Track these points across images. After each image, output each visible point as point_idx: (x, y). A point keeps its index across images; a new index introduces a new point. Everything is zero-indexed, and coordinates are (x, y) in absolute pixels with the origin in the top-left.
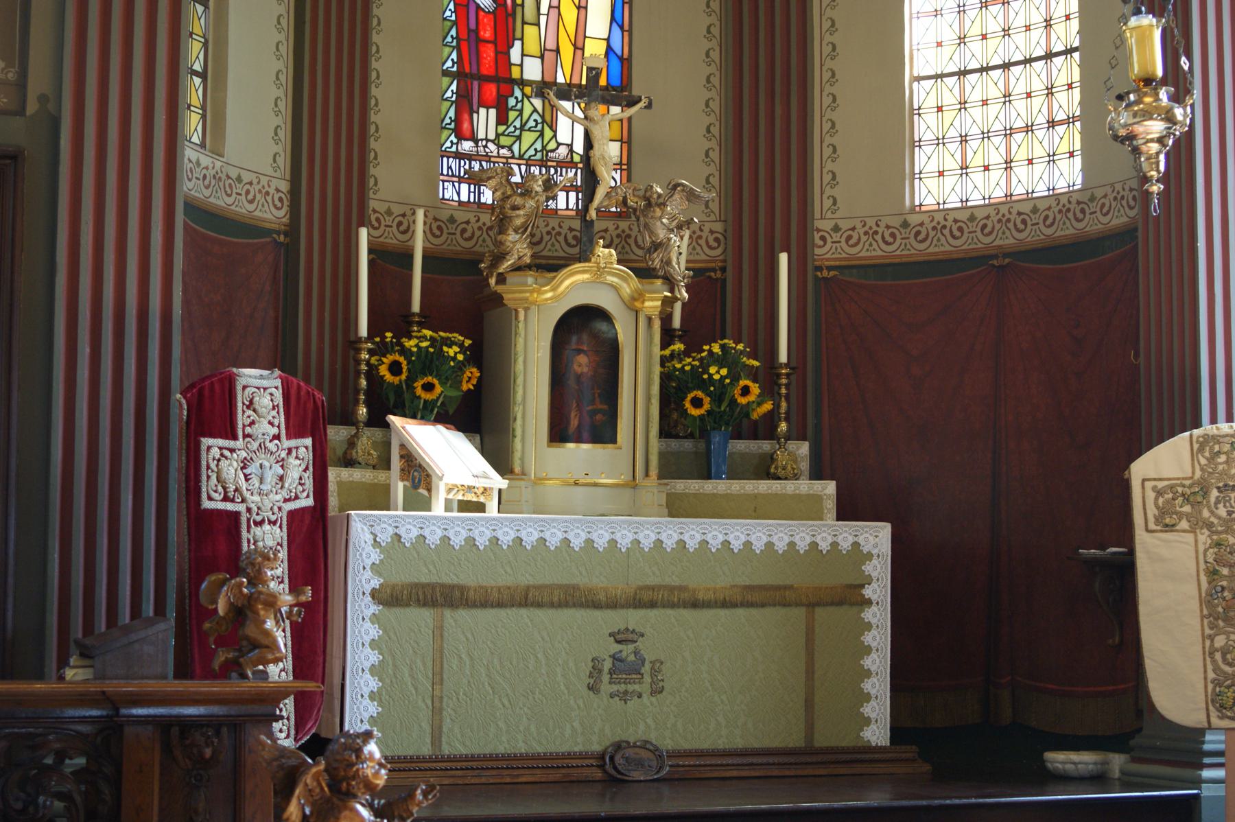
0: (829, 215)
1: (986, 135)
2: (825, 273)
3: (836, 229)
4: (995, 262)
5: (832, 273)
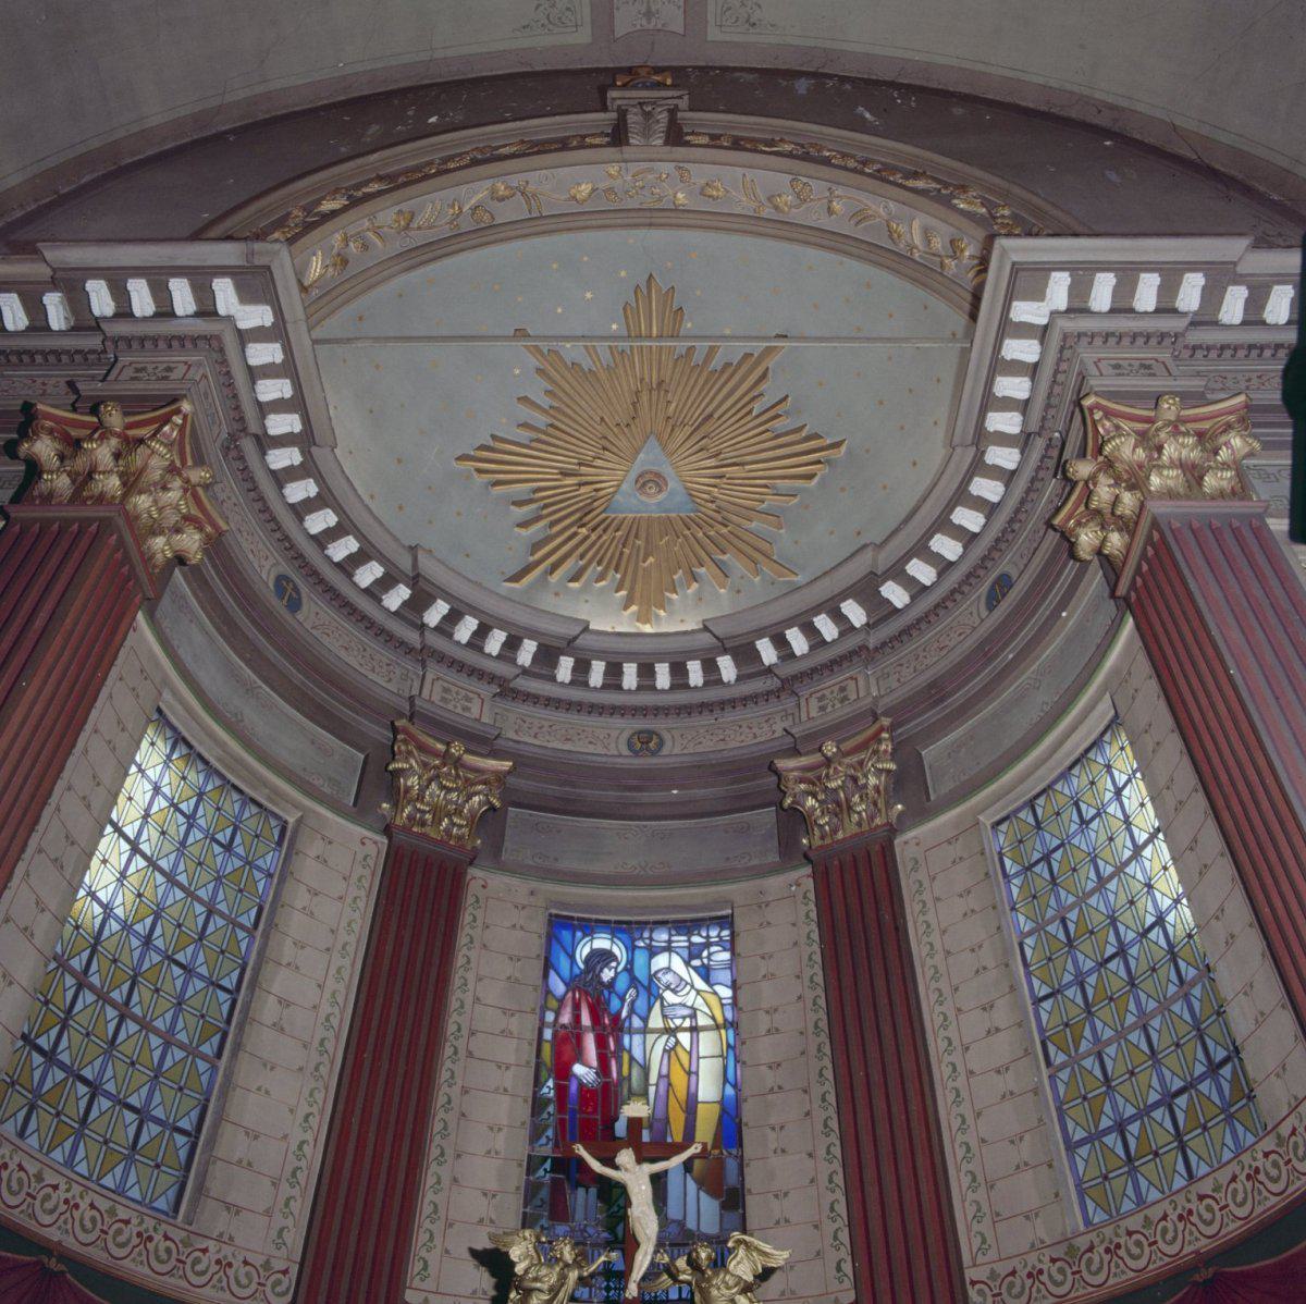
1: (1145, 1112)
3: (993, 1275)
4: (1197, 1277)
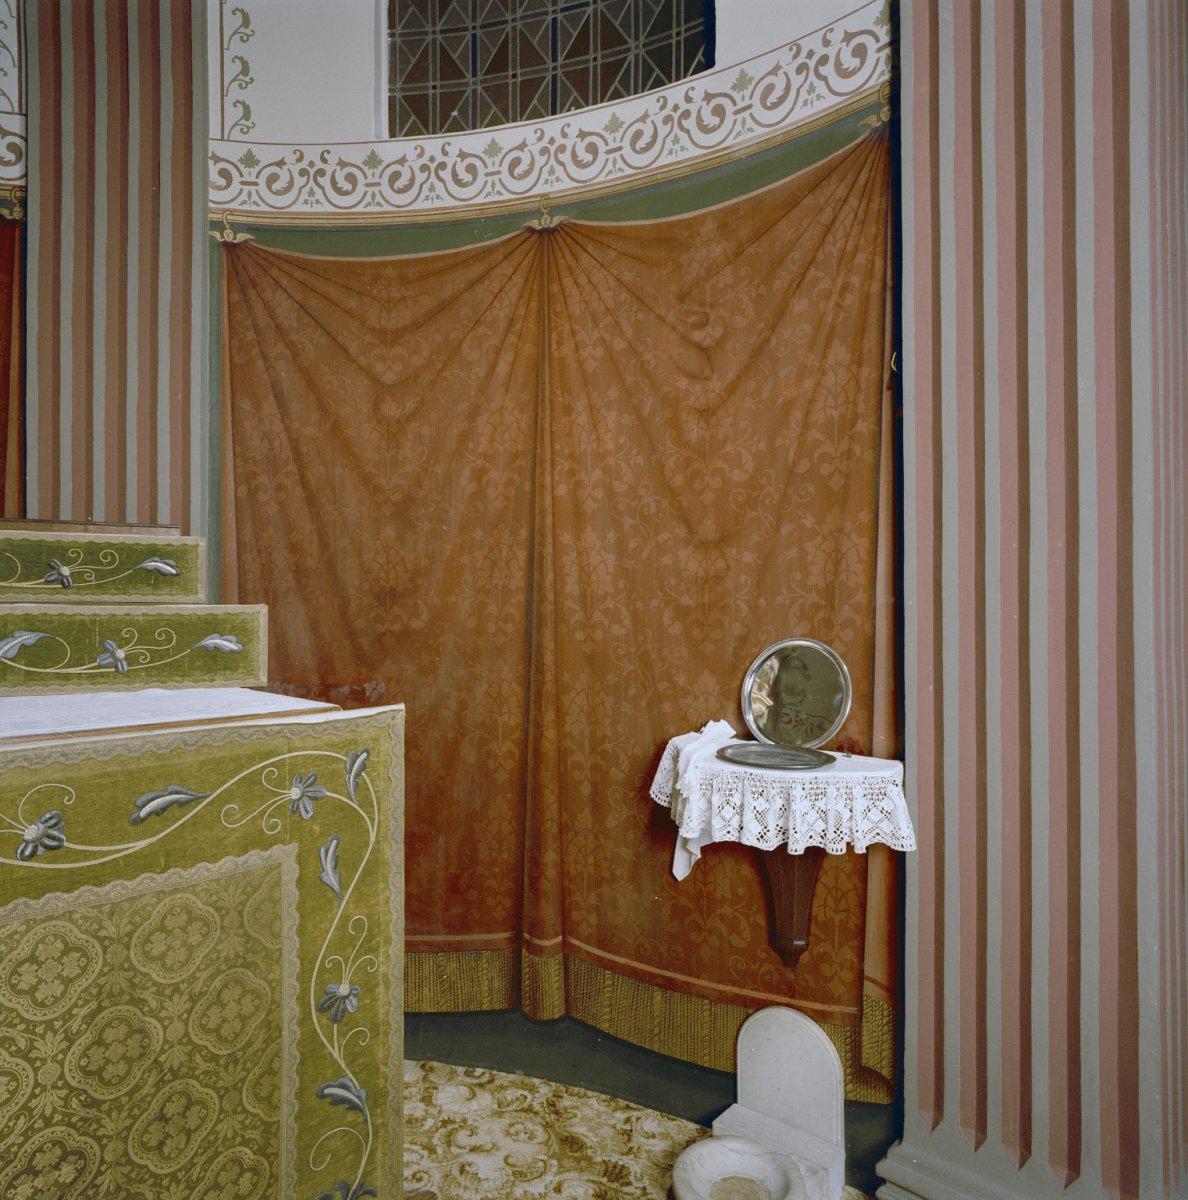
0: (236, 134)
2: (229, 236)
3: (250, 160)
4: (535, 224)
5: (241, 237)
